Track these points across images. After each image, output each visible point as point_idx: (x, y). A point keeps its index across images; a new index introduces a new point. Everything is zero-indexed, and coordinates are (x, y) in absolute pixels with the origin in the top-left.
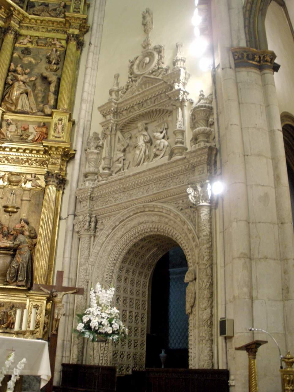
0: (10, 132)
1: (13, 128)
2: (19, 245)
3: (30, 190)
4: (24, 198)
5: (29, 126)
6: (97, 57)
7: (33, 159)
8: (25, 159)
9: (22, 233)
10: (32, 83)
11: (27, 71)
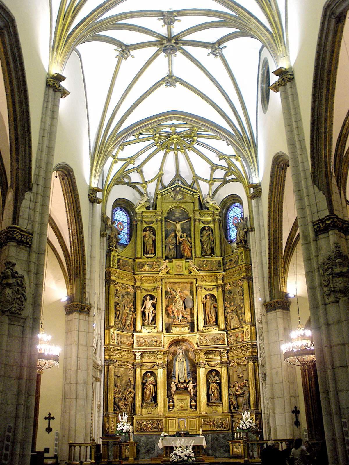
2: (244, 392)
8: (240, 351)
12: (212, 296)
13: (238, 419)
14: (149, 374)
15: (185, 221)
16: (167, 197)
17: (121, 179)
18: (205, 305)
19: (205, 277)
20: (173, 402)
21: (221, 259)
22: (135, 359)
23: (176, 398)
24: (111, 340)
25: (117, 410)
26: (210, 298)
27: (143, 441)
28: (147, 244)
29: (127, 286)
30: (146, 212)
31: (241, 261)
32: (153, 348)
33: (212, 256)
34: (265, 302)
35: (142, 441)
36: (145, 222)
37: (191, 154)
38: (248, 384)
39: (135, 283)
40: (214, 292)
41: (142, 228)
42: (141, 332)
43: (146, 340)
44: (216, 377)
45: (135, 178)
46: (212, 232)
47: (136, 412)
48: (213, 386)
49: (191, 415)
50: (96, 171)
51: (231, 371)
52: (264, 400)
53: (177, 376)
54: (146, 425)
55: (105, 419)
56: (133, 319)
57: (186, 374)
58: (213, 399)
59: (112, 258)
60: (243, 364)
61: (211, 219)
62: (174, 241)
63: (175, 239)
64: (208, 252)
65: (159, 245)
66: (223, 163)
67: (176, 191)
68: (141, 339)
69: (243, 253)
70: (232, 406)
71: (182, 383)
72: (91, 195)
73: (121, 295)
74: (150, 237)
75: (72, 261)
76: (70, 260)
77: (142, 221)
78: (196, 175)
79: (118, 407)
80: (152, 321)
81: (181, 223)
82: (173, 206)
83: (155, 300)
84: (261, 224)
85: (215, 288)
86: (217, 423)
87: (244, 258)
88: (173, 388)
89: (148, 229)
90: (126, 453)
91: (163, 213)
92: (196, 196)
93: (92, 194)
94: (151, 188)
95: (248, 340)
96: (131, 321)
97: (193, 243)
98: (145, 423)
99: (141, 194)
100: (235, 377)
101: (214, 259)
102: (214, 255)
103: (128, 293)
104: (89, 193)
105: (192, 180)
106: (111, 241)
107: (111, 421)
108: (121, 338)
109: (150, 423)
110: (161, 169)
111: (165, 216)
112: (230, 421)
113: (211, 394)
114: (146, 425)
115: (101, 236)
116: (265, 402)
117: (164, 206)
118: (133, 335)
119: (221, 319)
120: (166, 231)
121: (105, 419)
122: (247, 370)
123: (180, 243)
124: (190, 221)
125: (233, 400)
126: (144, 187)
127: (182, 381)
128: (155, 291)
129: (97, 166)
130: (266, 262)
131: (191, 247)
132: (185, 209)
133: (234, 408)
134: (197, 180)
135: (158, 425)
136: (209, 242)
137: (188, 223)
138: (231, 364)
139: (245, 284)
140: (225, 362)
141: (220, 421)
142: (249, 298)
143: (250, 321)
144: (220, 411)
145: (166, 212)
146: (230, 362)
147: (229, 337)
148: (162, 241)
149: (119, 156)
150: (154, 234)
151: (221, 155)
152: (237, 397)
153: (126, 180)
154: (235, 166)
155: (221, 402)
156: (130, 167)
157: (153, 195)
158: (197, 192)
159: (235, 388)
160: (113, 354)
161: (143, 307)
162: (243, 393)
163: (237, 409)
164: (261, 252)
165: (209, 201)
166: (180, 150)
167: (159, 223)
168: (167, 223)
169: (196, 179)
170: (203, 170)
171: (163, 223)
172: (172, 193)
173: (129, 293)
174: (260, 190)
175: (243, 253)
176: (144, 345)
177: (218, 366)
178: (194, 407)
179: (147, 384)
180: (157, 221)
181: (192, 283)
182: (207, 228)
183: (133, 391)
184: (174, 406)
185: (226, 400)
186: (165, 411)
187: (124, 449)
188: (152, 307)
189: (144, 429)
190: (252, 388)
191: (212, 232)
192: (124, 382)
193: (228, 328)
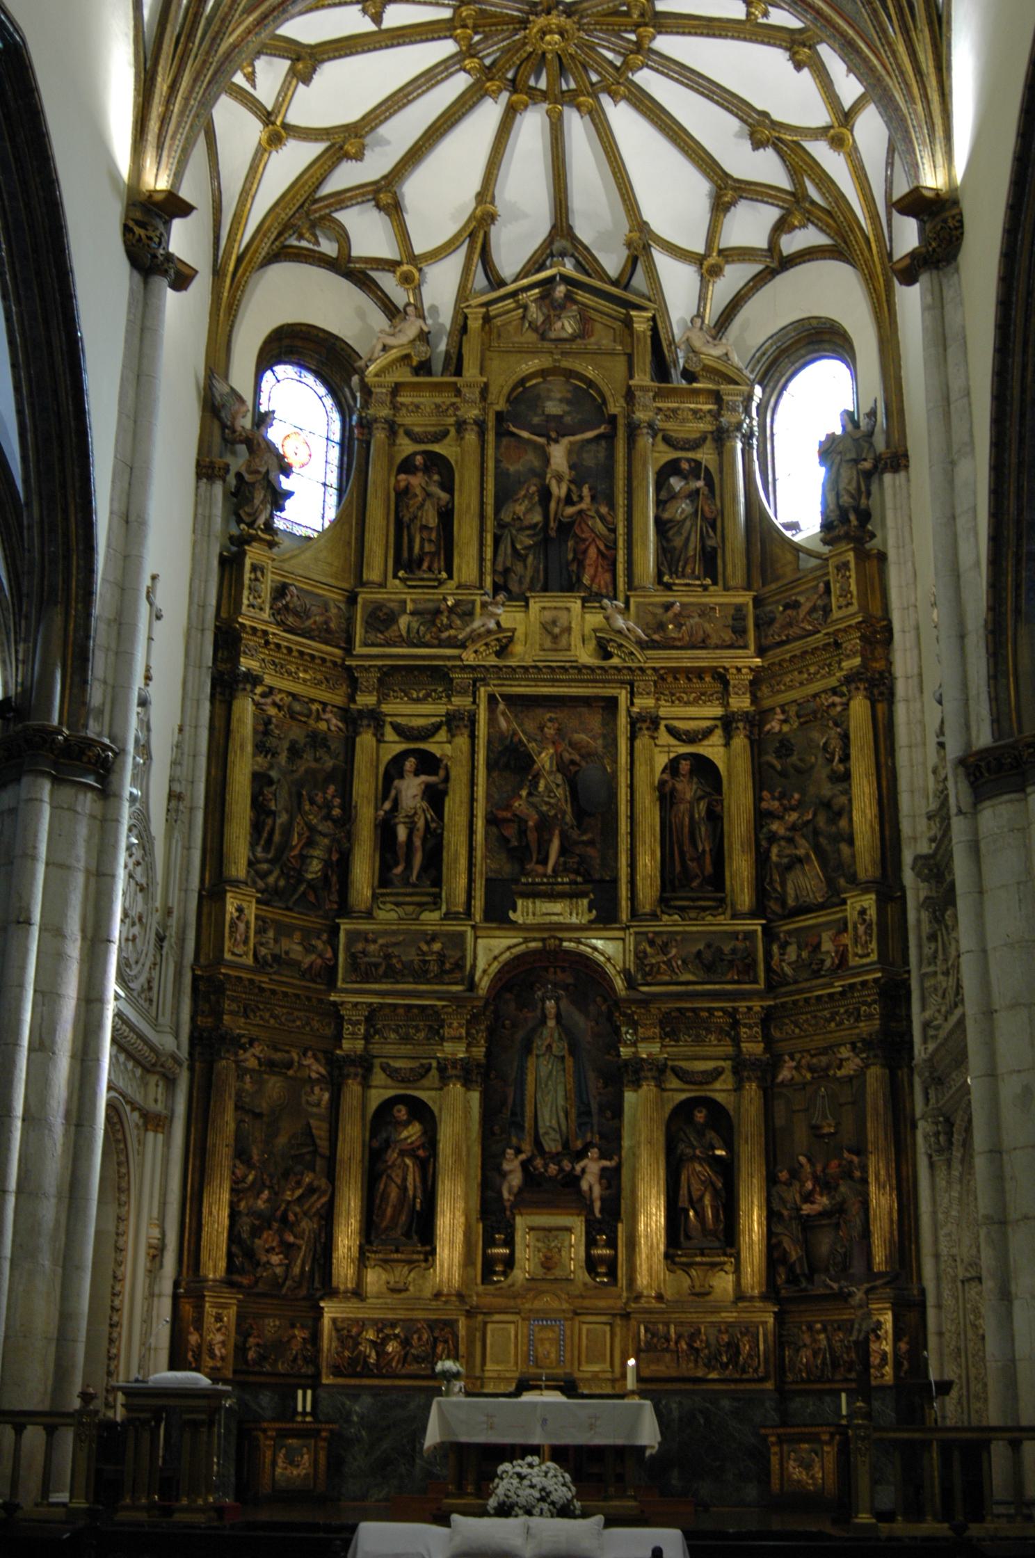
0: (789, 964)
1: (792, 953)
3: (850, 1079)
4: (842, 1100)
5: (820, 936)
6: (918, 705)
7: (842, 1010)
9: (851, 1177)
10: (810, 827)
11: (793, 802)
12: (703, 767)
13: (810, 1328)
14: (401, 1112)
15: (590, 435)
16: (511, 328)
17: (302, 227)
18: (666, 797)
19: (670, 679)
20: (510, 1242)
21: (745, 598)
22: (338, 1037)
23: (519, 1221)
24: (227, 944)
25: (241, 1271)
26: (692, 772)
27: (362, 1417)
28: (415, 528)
29: (315, 707)
30: (415, 387)
31: (843, 601)
32: (426, 995)
33: (705, 588)
34: (969, 743)
35: (355, 1418)
36: (408, 434)
37: (623, 119)
38: (864, 1168)
39: (352, 699)
40: (713, 749)
41: (391, 458)
42: (369, 915)
43: (396, 951)
44: (711, 1135)
45: (368, 234)
46: (710, 483)
47: (334, 1284)
49: (587, 1303)
50: (164, 120)
51: (780, 1107)
52: (936, 1241)
53: (528, 1124)
54: (379, 1346)
55: (187, 1309)
56: (335, 857)
57: (573, 1115)
59: (247, 575)
60: (839, 1074)
61: (705, 426)
62: (537, 517)
63: (538, 509)
64: (689, 570)
65: (466, 532)
66: (766, 168)
67: (553, 301)
68: (372, 948)
69: (852, 565)
70: (782, 1270)
71: (556, 1158)
72: (138, 230)
73: (286, 745)
74: (429, 495)
75: (30, 527)
76: (21, 526)
77: (392, 428)
78: (640, 226)
79: (250, 1254)
80: (424, 868)
81: (571, 443)
82: (532, 365)
83: (442, 773)
84: (956, 385)
85: (719, 732)
86: (708, 1346)
87: (853, 588)
88: (510, 1177)
89: (419, 460)
90: (278, 1471)
91: (492, 397)
92: (641, 323)
93: (143, 225)
94: (442, 286)
95: (865, 961)
96: (327, 864)
97: (621, 529)
98: (371, 1335)
99: (391, 310)
100: (801, 1135)
101: (716, 597)
102: (715, 583)
103: (317, 740)
104: (127, 217)
105: (625, 253)
106: (250, 500)
107: (209, 1320)
108: (276, 941)
109: (396, 1336)
110: (486, 194)
111: (498, 408)
112: (771, 1338)
114: (379, 1346)
115: (199, 476)
116: (944, 1250)
117: (495, 364)
118: (335, 931)
119: (740, 867)
120: (500, 475)
121: (187, 1309)
122: (858, 1101)
123: (566, 528)
124: (610, 437)
125: (787, 1243)
126: (406, 279)
127: (552, 1144)
128: (442, 735)
129: (169, 100)
130: (977, 564)
131: (613, 547)
132: (590, 383)
133: (793, 1280)
134: (647, 248)
135: (434, 1347)
136: (694, 524)
137: (603, 443)
138: (785, 1074)
139: (859, 707)
140: (755, 1064)
141: (726, 1338)
142: (873, 770)
143: (878, 874)
144: (725, 1290)
145: (506, 390)
146: (774, 1064)
147: (775, 948)
148: (482, 517)
149: (296, 116)
150: (448, 486)
151: (759, 123)
152: (807, 1225)
153: (328, 247)
154: (825, 182)
155: (729, 1251)
156: (346, 176)
157: (446, 317)
158: (647, 304)
159: (797, 1185)
160: (234, 1007)
161: (387, 806)
162: (838, 1211)
163: (804, 1284)
164: (954, 517)
165: (697, 344)
166: (570, 99)
167: (471, 437)
168: (505, 441)
169: (642, 241)
170: (672, 199)
171: (491, 437)
172: (533, 307)
173: (325, 739)
174: (951, 223)
175: (852, 565)
176: (385, 975)
178: (602, 1270)
179: (392, 1155)
180: (461, 425)
181: (612, 703)
182: (685, 466)
183: (323, 1183)
184: (509, 1262)
185: (755, 1237)
186: (466, 1281)
187: (269, 1454)
188: (425, 805)
189: (366, 1362)
190: (881, 1186)
191: (710, 483)
192: (282, 1140)
193: (774, 906)
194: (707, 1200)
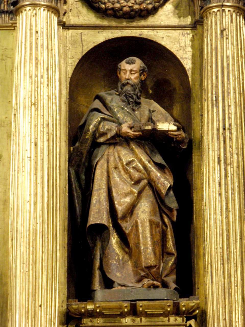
48: (123, 176)
58: (116, 275)
113: (100, 229)
155: (185, 303)
177: (166, 14)
194: (145, 211)
